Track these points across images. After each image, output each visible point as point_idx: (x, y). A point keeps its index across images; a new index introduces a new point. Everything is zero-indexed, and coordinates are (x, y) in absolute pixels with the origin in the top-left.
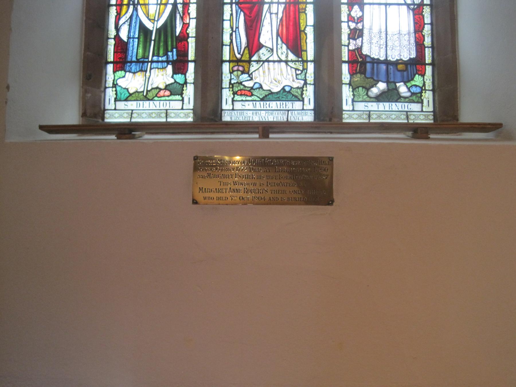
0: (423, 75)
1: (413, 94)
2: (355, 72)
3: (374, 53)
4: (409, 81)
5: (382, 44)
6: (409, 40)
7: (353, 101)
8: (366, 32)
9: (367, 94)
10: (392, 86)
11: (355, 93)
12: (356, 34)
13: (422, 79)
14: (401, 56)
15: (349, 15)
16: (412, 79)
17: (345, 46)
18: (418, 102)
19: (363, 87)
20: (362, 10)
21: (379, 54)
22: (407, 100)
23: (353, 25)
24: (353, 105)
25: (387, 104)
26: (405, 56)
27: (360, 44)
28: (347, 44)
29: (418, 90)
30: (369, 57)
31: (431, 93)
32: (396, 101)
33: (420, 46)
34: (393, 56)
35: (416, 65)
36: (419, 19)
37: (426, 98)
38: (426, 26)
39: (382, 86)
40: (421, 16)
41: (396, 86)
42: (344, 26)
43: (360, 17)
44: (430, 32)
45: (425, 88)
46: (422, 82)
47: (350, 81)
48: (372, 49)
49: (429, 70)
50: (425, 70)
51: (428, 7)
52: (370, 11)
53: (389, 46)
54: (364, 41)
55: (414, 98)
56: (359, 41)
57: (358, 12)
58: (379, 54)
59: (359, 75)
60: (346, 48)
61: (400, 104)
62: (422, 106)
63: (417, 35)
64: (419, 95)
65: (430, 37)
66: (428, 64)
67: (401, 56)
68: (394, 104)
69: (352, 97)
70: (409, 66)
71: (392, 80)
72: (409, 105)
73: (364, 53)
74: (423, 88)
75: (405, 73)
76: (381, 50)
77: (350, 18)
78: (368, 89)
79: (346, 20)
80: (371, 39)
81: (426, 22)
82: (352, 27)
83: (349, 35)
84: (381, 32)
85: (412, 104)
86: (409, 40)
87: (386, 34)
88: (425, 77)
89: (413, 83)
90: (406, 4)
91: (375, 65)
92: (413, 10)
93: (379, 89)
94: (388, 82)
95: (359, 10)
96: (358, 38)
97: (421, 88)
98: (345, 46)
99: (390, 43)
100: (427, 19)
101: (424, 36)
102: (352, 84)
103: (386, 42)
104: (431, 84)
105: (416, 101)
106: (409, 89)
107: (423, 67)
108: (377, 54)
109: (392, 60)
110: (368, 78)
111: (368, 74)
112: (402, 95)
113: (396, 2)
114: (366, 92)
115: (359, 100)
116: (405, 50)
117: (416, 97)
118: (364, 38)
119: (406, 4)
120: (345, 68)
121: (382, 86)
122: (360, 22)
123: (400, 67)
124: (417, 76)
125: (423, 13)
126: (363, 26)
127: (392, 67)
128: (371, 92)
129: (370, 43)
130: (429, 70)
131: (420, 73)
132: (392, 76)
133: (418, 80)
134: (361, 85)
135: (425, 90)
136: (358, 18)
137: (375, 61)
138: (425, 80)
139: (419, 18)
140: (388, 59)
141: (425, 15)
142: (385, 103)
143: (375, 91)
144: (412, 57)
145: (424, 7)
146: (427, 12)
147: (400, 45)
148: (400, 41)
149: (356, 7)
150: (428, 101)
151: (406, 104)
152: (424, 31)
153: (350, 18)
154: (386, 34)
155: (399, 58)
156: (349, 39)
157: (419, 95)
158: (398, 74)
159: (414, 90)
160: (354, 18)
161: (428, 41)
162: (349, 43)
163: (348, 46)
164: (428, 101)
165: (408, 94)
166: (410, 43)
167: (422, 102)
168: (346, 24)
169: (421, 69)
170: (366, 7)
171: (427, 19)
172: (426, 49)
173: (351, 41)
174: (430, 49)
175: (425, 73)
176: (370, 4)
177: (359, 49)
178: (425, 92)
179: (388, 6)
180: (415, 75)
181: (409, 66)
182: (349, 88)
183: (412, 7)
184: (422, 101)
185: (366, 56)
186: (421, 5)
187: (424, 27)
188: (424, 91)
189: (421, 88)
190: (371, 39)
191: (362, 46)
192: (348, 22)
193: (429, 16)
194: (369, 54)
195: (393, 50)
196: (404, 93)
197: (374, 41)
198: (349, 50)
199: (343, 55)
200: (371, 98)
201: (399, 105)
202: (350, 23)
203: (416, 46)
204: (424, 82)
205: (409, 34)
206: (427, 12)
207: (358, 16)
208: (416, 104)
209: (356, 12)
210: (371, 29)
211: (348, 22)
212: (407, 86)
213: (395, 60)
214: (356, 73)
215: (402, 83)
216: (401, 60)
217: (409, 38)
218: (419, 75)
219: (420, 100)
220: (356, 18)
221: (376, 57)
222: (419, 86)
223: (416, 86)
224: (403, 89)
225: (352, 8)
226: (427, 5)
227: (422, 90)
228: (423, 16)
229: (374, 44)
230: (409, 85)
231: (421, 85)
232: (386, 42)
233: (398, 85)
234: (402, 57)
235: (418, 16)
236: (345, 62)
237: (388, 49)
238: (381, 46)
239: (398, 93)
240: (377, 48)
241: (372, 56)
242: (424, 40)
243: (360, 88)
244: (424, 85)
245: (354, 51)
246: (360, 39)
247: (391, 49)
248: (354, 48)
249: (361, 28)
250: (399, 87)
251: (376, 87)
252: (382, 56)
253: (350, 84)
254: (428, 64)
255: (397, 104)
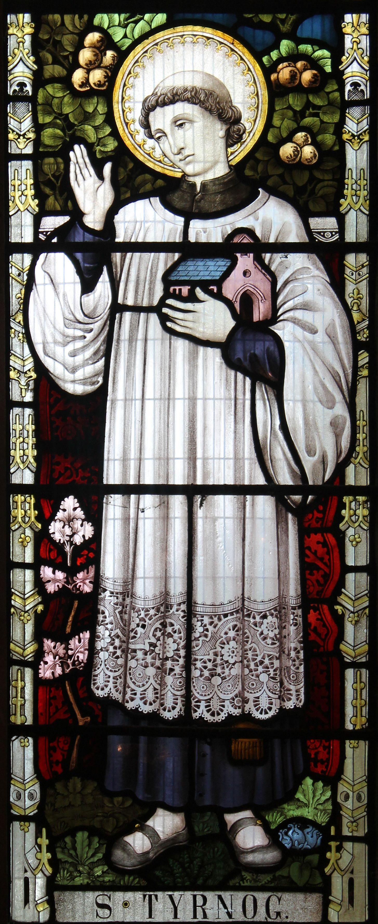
0: (332, 778)
1: (289, 855)
2: (59, 770)
3: (139, 691)
4: (275, 804)
5: (170, 654)
6: (280, 639)
7: (52, 886)
8: (108, 604)
9: (108, 860)
10: (205, 825)
11: (60, 856)
12: (70, 613)
13: (329, 794)
14: (245, 701)
15: (42, 538)
16: (290, 797)
17: (23, 664)
18: (307, 889)
19: (93, 832)
20: (94, 516)
21: (159, 696)
22: (265, 879)
23: (54, 578)
24: (51, 902)
25: (185, 899)
26: (264, 703)
27: (83, 657)
28: (30, 658)
29: (312, 838)
30: (120, 706)
31: (361, 850)
32: (223, 886)
33: (322, 660)
34: (216, 702)
35: (302, 739)
36: (321, 551)
37: (343, 872)
38: (350, 577)
39: (165, 823)
40: (331, 539)
41: (224, 823)
42: (23, 580)
43: (86, 543)
44: (365, 602)
45: (339, 829)
46: (329, 806)
47: (41, 807)
48: (132, 677)
49: (356, 759)
50: (343, 757)
51: (361, 499)
52: (126, 520)
53: (199, 664)
54: (100, 645)
55: (293, 871)
56: (78, 646)
57: (77, 524)
58: (159, 696)
59: (77, 783)
60: (28, 672)
61: (240, 895)
62: (326, 904)
63: (312, 616)
64: (315, 858)
65: (364, 622)
66: (355, 735)
67: (245, 701)
68: (211, 896)
69: (49, 871)
70: (277, 742)
71: (208, 801)
72: (274, 900)
73: (100, 693)
74: (330, 832)
75: (260, 772)
76: (169, 679)
77: (48, 551)
78: (113, 839)
79: (29, 558)
80: (127, 633)
81: (350, 562)
82: (51, 588)
83: (39, 619)
84: (168, 607)
85: (287, 896)
86: (280, 639)
87: (190, 614)
88: (342, 788)
89: (293, 811)
90: (270, 488)
91: (143, 740)
92: (300, 512)
93: (153, 834)
94: (187, 808)
95: (79, 513)
96: (76, 632)
97: (323, 830)
98: (23, 664)
99: (202, 653)
100: (356, 554)
101: (340, 620)
102: (50, 820)
103: (188, 647)
104: (362, 813)
105: (300, 883)
106: (273, 835)
107: (335, 744)
108: (150, 695)
109: (207, 717)
110: (111, 795)
111: (114, 779)
112: (250, 858)
113: (230, 481)
114: (103, 850)
115: (78, 881)
116: (264, 678)
117: (300, 869)
118: (100, 629)
119: (270, 488)
120: (23, 755)
121: (165, 823)
122: (84, 567)
123: (241, 745)
124: (309, 781)
125: (342, 526)
126: (97, 581)
127: (207, 749)
128: (125, 847)
129: (125, 651)
130: (356, 759)
131: (320, 769)
132: (208, 783)
133: (311, 799)
134: (87, 822)
135: (341, 838)
136: (77, 550)
137: (144, 724)
138: (340, 799)
139: (325, 544)
140: (196, 715)
141: (350, 532)
142: (176, 895)
143: (138, 842)
144: (290, 705)
145: (346, 499)
146: (355, 515)
147: (244, 657)
148: (244, 642)
149: (70, 503)
150: (351, 882)
151: (262, 897)
152: (342, 599)
153: (48, 551)
154: (190, 614)
155: (236, 712)
156: (38, 637)
157: (315, 858)
158: (232, 775)
159: (293, 837)
160: (59, 547)
161: (355, 638)
162: (39, 654)
163: (35, 665)
164: (351, 882)
165: (270, 856)
166: (282, 651)
167: (325, 889)
168: (29, 574)
169: (323, 755)
170: (113, 507)
171: (356, 554)
172: (350, 673)
173: (48, 644)
174: (365, 673)
175: (341, 770)
176: (125, 490)
177: (82, 675)
178: (339, 849)
179: (198, 498)
180: (298, 782)
181: (277, 742)
182: (38, 834)
183: (297, 498)
184: (327, 881)
185: (108, 701)
186: (335, 489)
187: (342, 583)
188: (333, 844)
189: (323, 830)
190: (127, 633)
191: (91, 664)
192: (35, 567)
193: (364, 537)
194: (117, 696)
195: (216, 680)
196: (254, 850)
197: (140, 645)
198: (37, 681)
199: (16, 701)
200: (121, 872)
201: (235, 899)
202: (47, 572)
203: (307, 661)
204: (337, 808)
205: (280, 610)
206: (355, 515)
207: (78, 540)
208: (300, 896)
209: (69, 524)
210: (127, 592)
211: (35, 567)
212: (266, 827)
213: (223, 716)
214: (66, 776)
215: (248, 814)
216: (246, 717)
217: (281, 628)
218: (315, 780)
219: (319, 880)
220: (68, 549)
221: (146, 709)
222: (314, 824)
223: (302, 823)
224: (251, 837)
225: (56, 508)
226: (355, 491)
227: (327, 838)
228: (341, 537)
229: (140, 655)
230: (275, 819)
231: (322, 819)
232: (188, 647)
233: (231, 818)
234: (250, 707)
235: (319, 537)
236: (23, 731)
237: (196, 673)
238: (169, 664)
239: (233, 852)
240: (151, 671)
241: (130, 705)
242: (341, 637)
243: (81, 836)
244: (336, 817)
245: (56, 682)
246: (87, 635)
247: (206, 673)
248: (59, 671)
249: (87, 588)
250: (237, 826)
251: (143, 829)
252: (169, 702)
253: (39, 820)
254: (355, 735)
255: (226, 895)
